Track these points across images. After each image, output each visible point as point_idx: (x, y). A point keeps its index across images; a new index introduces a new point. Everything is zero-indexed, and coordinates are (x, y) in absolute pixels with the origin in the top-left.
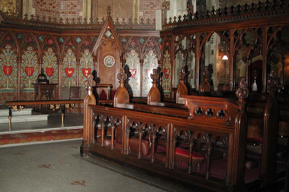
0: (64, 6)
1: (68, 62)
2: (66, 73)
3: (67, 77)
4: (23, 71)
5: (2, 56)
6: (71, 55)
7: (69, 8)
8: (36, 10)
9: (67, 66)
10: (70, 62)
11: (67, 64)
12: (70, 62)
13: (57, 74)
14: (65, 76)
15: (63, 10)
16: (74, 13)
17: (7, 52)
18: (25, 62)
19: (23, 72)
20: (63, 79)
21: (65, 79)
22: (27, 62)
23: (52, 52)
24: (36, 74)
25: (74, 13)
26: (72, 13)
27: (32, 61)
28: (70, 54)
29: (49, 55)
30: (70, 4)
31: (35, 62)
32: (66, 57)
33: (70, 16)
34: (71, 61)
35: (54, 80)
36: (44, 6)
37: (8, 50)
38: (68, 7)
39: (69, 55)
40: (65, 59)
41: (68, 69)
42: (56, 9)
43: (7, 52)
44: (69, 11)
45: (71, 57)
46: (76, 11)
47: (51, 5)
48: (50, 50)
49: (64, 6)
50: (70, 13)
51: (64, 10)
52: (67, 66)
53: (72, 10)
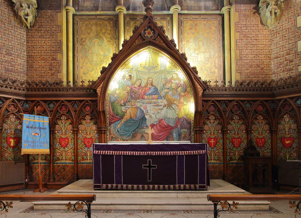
0: (275, 65)
1: (284, 129)
2: (282, 143)
3: (284, 148)
4: (229, 142)
5: (206, 128)
6: (289, 121)
7: (282, 66)
8: (241, 75)
9: (283, 135)
10: (287, 130)
11: (284, 132)
12: (287, 130)
13: (270, 145)
14: (280, 147)
15: (274, 70)
16: (290, 71)
17: (211, 123)
18: (230, 132)
19: (229, 144)
20: (278, 150)
21: (280, 151)
22: (233, 132)
23: (262, 120)
24: (244, 145)
25: (290, 70)
26: (287, 71)
27: (239, 131)
28: (287, 120)
29: (259, 123)
30: (284, 61)
31: (242, 132)
32: (282, 124)
33: (285, 75)
34: (290, 129)
35: (266, 152)
36: (251, 69)
37: (212, 121)
38: (280, 65)
39: (285, 121)
40: (281, 127)
41: (285, 137)
42: (265, 71)
43: (211, 123)
44: (283, 69)
45: (289, 124)
46: (293, 67)
47: (259, 67)
48: (260, 118)
49: (275, 65)
50: (283, 71)
51: (275, 70)
52: (283, 135)
53: (287, 67)
